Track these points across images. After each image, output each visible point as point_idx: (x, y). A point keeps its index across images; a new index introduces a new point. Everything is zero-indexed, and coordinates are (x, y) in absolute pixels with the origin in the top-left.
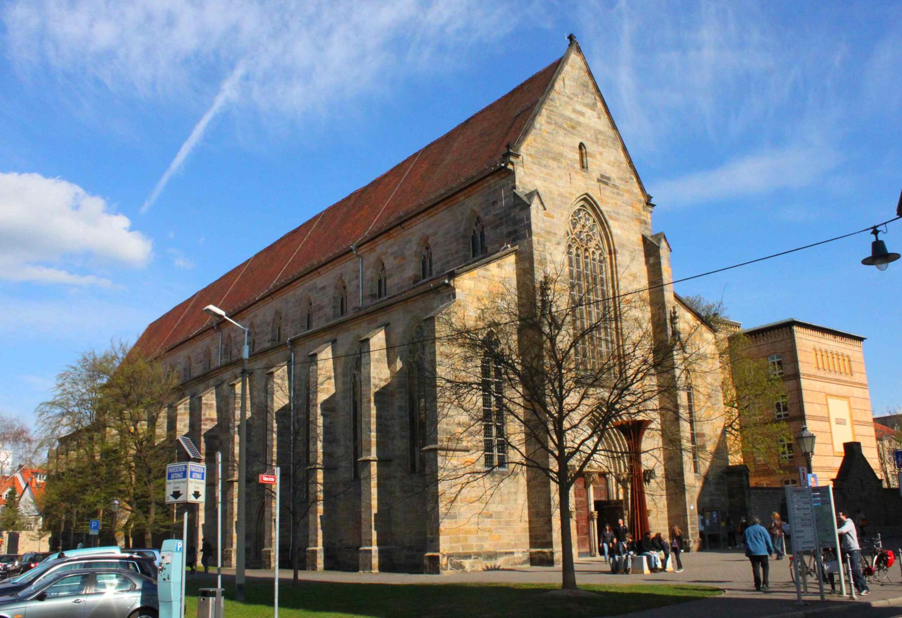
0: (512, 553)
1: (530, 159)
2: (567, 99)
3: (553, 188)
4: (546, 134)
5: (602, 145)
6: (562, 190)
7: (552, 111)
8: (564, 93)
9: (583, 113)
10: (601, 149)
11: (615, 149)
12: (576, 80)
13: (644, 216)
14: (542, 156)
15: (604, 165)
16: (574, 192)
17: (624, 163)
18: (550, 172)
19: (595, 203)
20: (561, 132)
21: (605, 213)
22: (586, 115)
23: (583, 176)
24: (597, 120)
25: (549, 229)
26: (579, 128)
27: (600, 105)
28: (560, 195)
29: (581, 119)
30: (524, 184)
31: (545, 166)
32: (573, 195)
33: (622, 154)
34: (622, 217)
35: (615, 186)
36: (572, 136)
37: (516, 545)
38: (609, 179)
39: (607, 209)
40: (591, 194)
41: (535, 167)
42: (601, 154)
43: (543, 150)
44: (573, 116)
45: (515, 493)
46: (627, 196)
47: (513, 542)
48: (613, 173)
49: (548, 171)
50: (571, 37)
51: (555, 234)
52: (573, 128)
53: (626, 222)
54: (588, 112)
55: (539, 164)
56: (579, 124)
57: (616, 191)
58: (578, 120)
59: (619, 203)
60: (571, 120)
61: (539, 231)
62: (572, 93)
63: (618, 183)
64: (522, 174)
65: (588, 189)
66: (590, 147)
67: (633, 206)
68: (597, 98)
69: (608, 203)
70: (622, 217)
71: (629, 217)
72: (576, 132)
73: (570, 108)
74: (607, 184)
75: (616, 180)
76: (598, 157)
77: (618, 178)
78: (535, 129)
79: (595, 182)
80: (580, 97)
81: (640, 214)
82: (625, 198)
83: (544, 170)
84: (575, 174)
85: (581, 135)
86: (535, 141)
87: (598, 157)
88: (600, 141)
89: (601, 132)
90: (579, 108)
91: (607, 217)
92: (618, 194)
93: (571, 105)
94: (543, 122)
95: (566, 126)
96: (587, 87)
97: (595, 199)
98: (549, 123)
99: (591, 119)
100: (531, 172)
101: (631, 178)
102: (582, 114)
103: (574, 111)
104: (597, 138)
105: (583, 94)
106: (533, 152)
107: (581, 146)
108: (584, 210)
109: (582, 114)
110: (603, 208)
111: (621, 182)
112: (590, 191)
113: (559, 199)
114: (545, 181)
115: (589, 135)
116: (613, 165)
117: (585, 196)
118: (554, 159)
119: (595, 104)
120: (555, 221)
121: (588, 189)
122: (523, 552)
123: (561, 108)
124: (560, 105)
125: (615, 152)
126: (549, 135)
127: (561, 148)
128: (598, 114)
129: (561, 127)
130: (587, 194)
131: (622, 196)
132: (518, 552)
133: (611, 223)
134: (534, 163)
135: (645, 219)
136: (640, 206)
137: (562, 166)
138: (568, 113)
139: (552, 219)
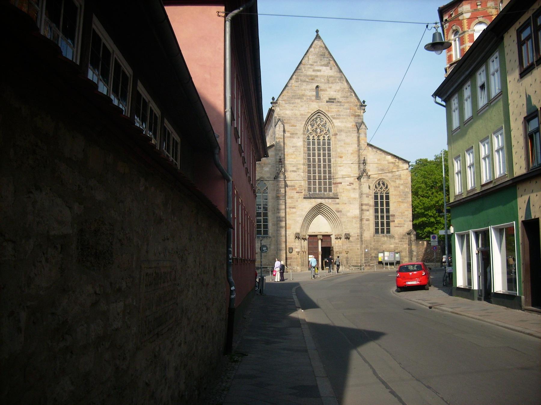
0: (267, 268)
1: (284, 102)
2: (309, 66)
3: (297, 112)
4: (295, 88)
5: (332, 83)
6: (302, 112)
7: (299, 75)
8: (308, 64)
9: (320, 70)
10: (330, 85)
11: (341, 82)
12: (317, 54)
13: (358, 112)
14: (292, 99)
15: (332, 93)
16: (310, 111)
17: (346, 88)
18: (296, 105)
19: (325, 113)
20: (305, 84)
21: (330, 117)
22: (322, 70)
23: (317, 102)
24: (330, 71)
25: (293, 132)
26: (316, 79)
27: (332, 62)
28: (302, 115)
29: (318, 73)
30: (280, 115)
31: (293, 103)
32: (309, 113)
33: (346, 84)
34: (342, 117)
35: (338, 102)
36: (312, 84)
37: (269, 265)
38: (335, 99)
39: (332, 114)
40: (321, 110)
41: (286, 105)
42: (330, 88)
43: (292, 96)
44: (313, 73)
45: (270, 245)
46: (346, 105)
47: (267, 264)
48: (338, 96)
49: (294, 105)
50: (317, 31)
51: (297, 134)
52: (312, 79)
53: (345, 118)
54: (324, 68)
55: (290, 103)
56: (317, 76)
57: (339, 104)
58: (316, 74)
59: (340, 110)
60: (311, 76)
61: (280, 136)
62: (313, 62)
63: (340, 100)
64: (279, 110)
65: (320, 107)
66: (322, 86)
67: (350, 109)
68: (331, 59)
69: (333, 111)
70: (342, 117)
71: (347, 115)
72: (313, 81)
73: (311, 70)
74: (333, 102)
75: (340, 98)
76: (328, 89)
77: (341, 97)
78: (288, 87)
79: (325, 103)
80: (318, 62)
81: (355, 112)
82: (345, 107)
83: (292, 105)
84: (312, 102)
85: (317, 82)
86: (287, 93)
87: (328, 89)
88: (330, 81)
89: (331, 77)
90: (317, 68)
91: (332, 119)
92: (340, 105)
93: (312, 68)
94: (293, 82)
95: (308, 80)
96: (325, 55)
97: (324, 111)
98: (297, 82)
99: (325, 71)
100: (284, 108)
101: (351, 95)
102: (320, 71)
103: (314, 71)
104: (329, 80)
105: (321, 60)
106: (286, 98)
107: (317, 87)
108: (319, 118)
109: (320, 71)
110: (329, 115)
111: (343, 99)
112: (321, 108)
113: (301, 116)
114: (292, 110)
115: (323, 80)
116: (339, 91)
117: (319, 111)
118: (299, 98)
119: (329, 63)
120: (297, 127)
121: (320, 107)
122: (272, 267)
123: (305, 72)
124: (305, 70)
125: (340, 84)
126: (296, 88)
127: (304, 92)
128: (330, 68)
129: (304, 81)
130: (319, 110)
131: (343, 106)
132: (269, 267)
133: (334, 121)
134: (286, 104)
135: (359, 114)
136: (356, 108)
137: (304, 100)
138: (310, 73)
139: (295, 127)
